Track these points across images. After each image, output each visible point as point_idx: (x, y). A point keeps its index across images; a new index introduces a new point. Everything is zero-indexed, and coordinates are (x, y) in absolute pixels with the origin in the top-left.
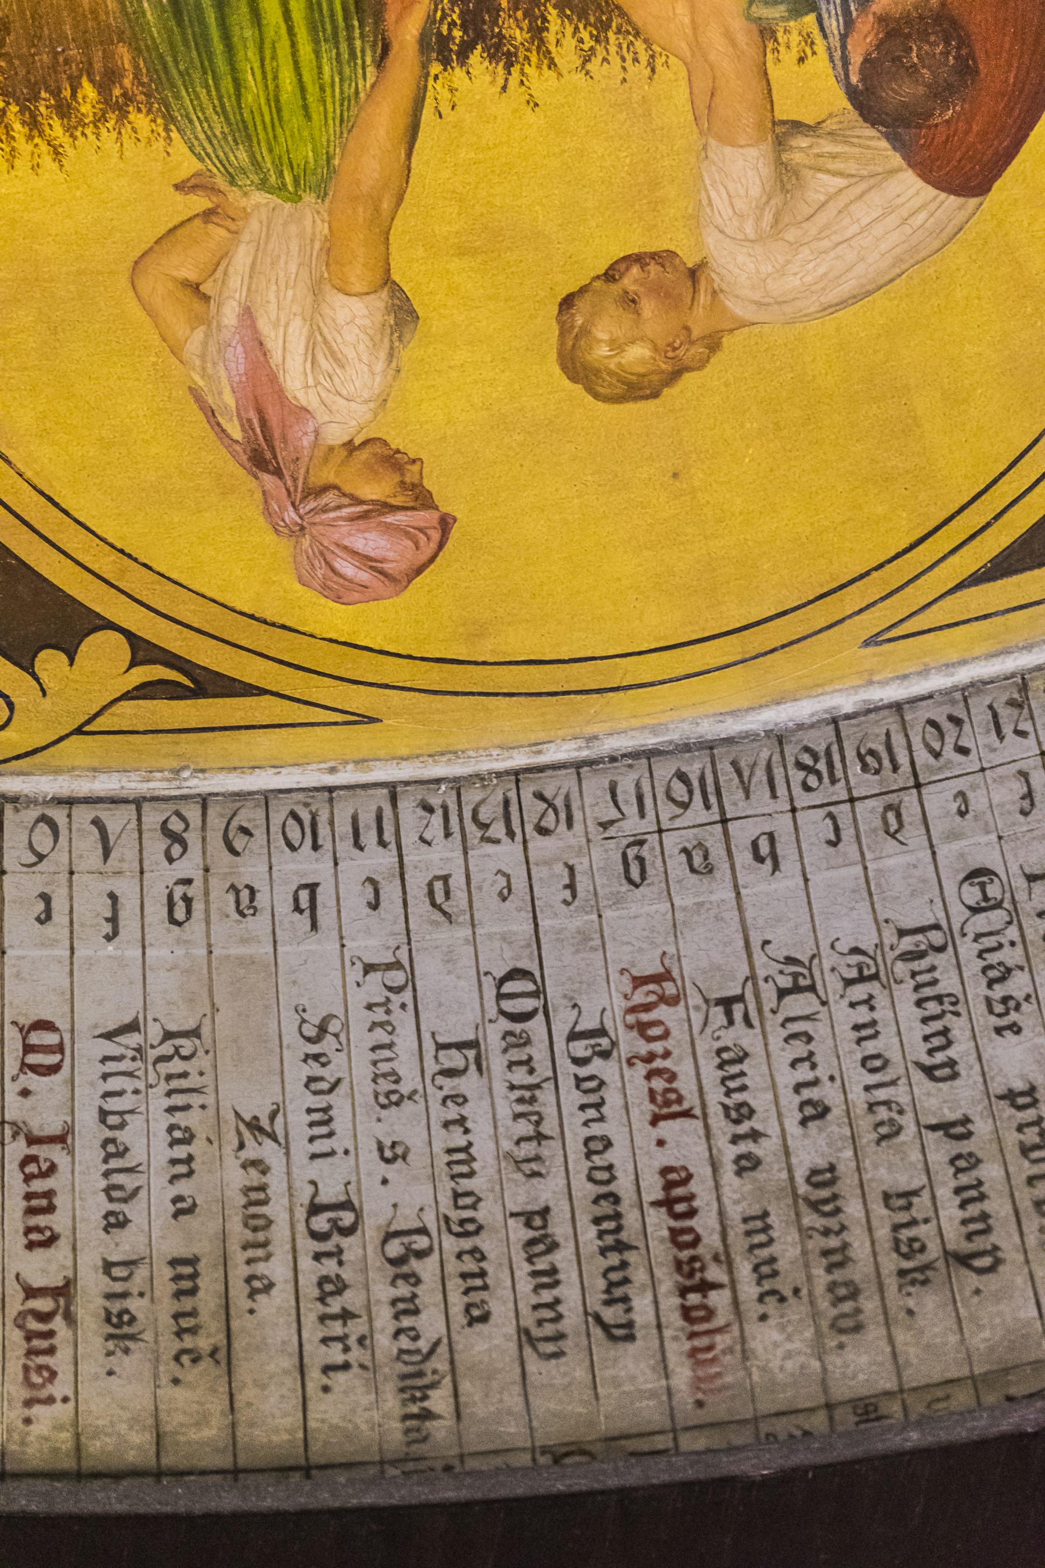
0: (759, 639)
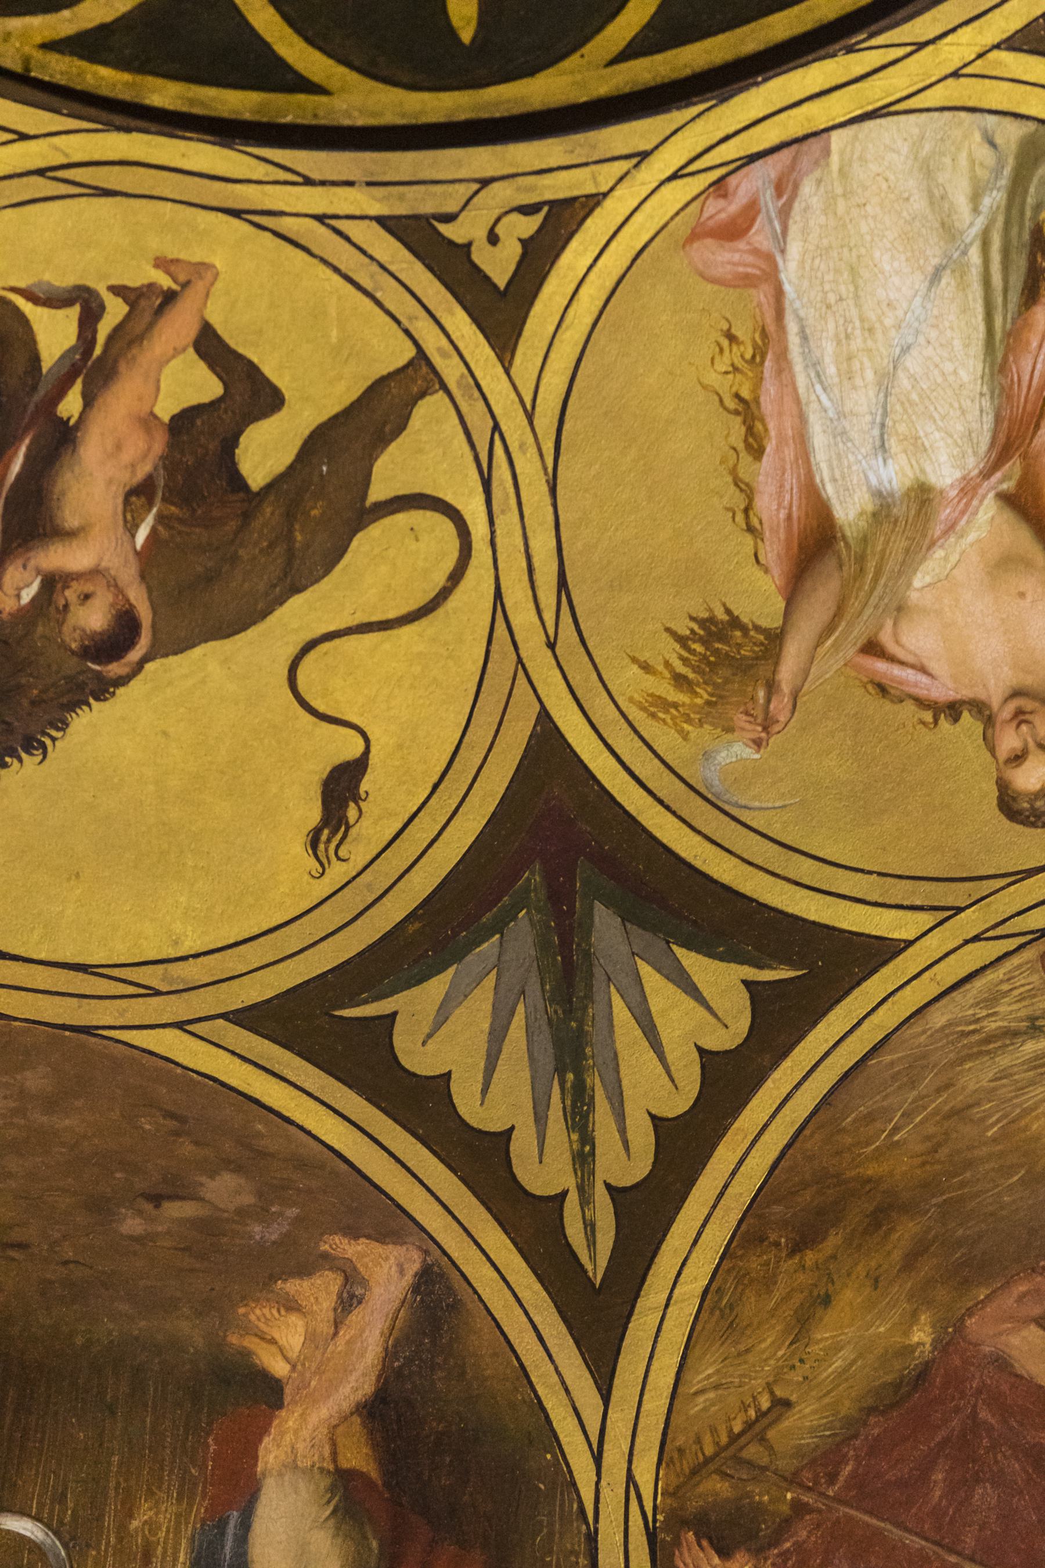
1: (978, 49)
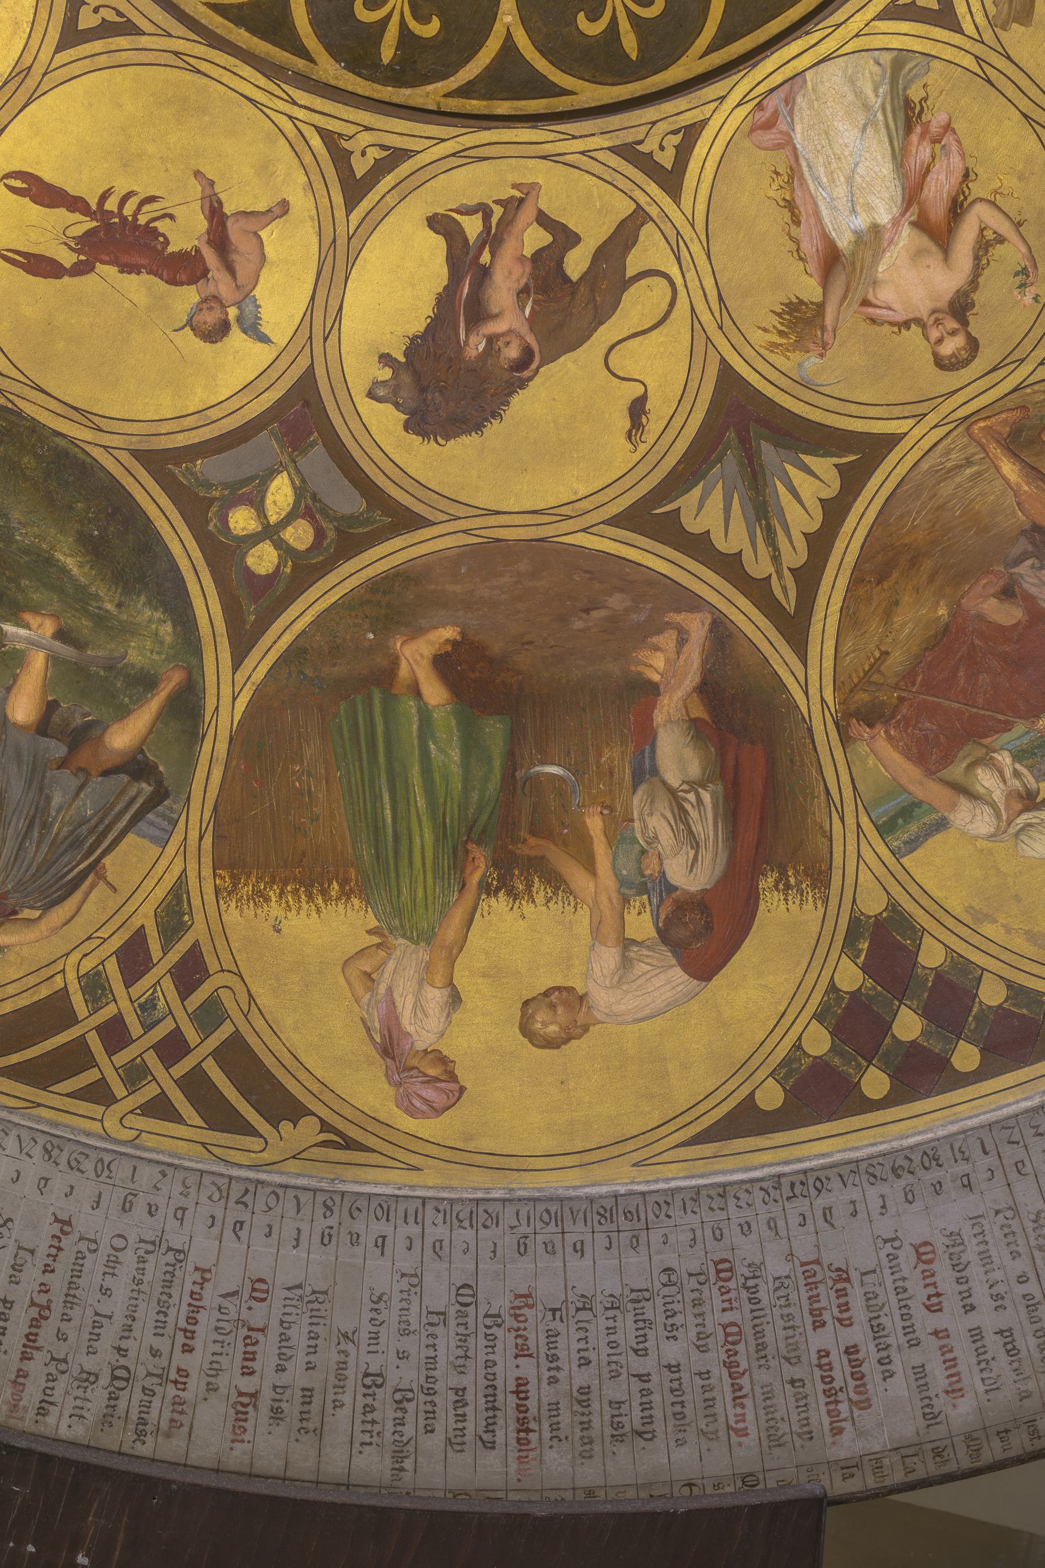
0: (586, 1157)
1: (865, 22)
